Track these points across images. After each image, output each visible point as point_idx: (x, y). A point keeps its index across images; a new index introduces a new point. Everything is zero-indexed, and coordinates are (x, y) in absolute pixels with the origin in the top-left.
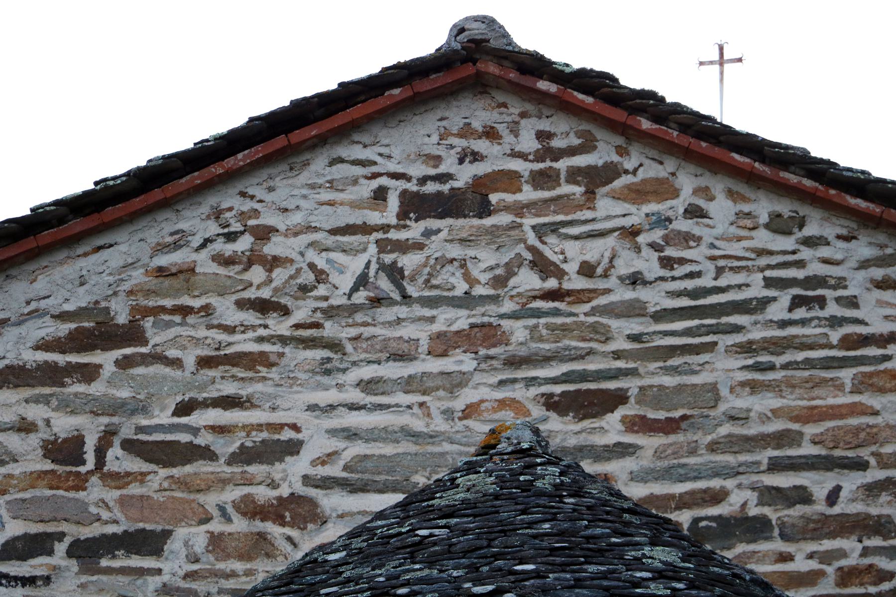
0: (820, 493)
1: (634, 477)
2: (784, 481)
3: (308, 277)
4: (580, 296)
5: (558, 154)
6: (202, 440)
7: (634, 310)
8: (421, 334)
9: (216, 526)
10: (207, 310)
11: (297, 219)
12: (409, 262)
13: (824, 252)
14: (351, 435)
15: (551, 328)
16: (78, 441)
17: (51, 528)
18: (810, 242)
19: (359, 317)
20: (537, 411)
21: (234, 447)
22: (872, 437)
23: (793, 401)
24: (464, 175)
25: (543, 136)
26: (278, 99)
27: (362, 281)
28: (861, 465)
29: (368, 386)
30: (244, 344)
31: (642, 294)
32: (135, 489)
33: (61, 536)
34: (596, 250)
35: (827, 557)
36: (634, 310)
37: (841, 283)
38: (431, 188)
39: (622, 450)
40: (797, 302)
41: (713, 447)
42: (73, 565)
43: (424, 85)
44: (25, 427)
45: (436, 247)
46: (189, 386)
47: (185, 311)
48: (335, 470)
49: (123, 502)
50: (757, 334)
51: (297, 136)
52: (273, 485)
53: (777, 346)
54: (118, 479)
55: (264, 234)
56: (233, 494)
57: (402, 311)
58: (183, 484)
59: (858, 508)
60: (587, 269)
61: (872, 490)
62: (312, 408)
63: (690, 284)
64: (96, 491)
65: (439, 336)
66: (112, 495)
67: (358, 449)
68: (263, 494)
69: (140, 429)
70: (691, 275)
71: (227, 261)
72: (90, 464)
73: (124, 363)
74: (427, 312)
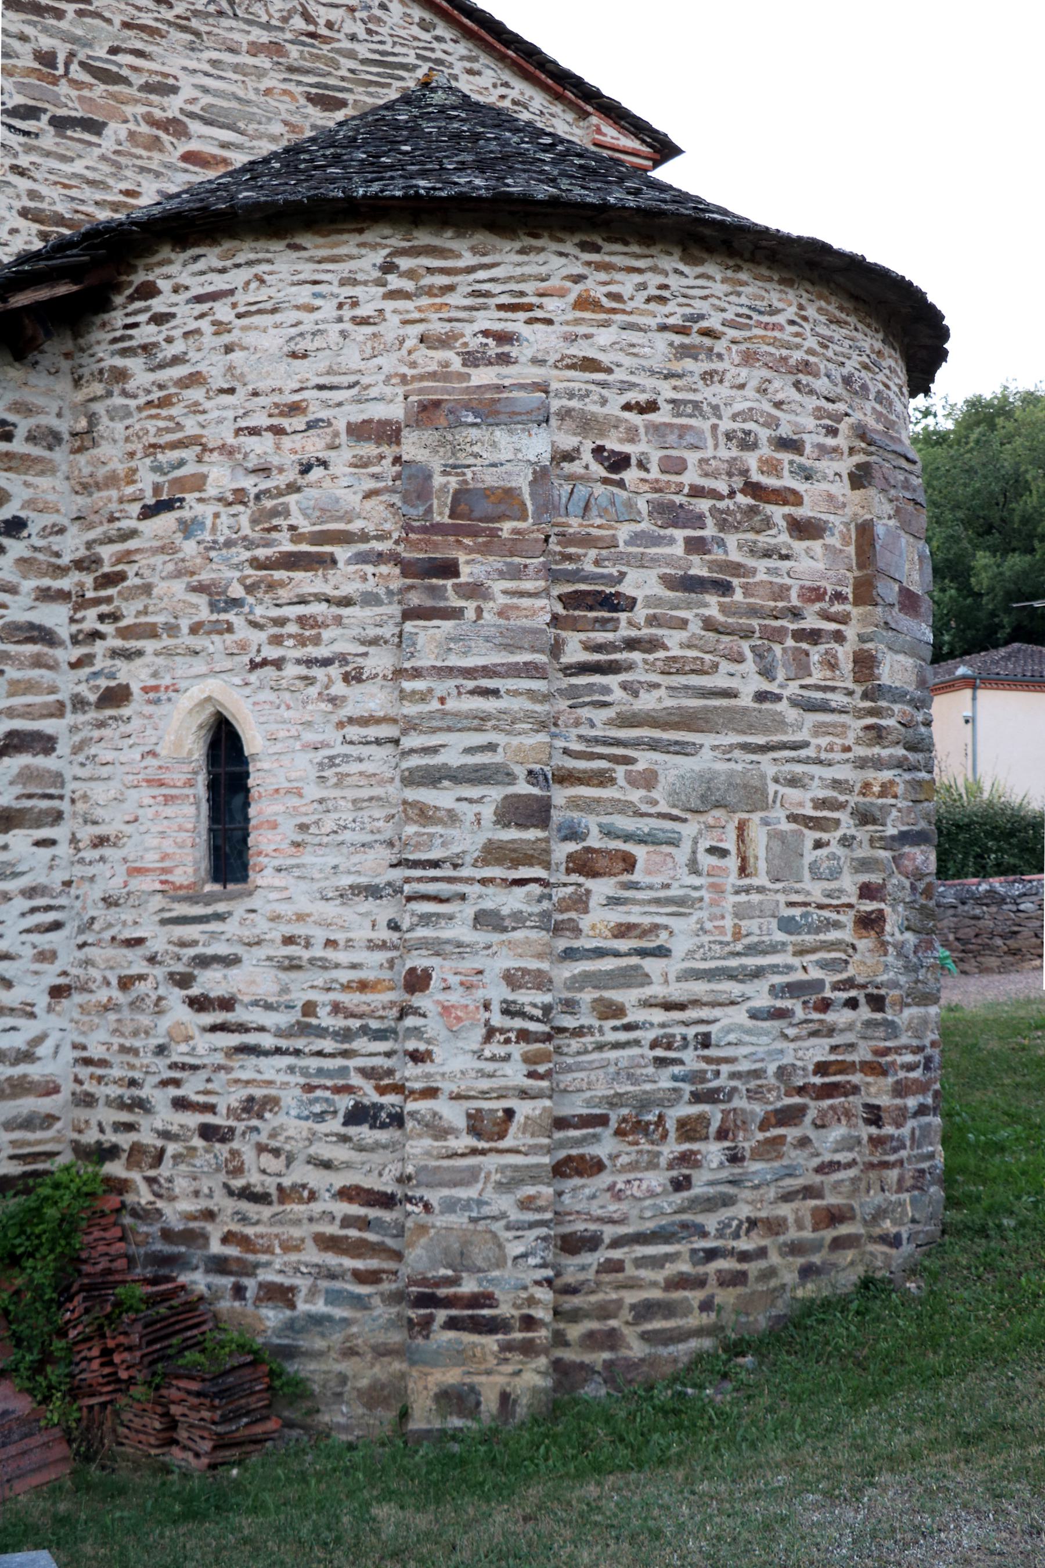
4: (326, 40)
6: (125, 72)
7: (351, 55)
8: (244, 40)
9: (132, 126)
13: (444, 46)
14: (206, 90)
15: (311, 54)
17: (39, 104)
18: (439, 39)
19: (211, 21)
20: (303, 101)
21: (142, 81)
29: (214, 63)
30: (146, 19)
31: (355, 46)
32: (86, 93)
33: (45, 111)
34: (335, 15)
36: (351, 55)
42: (51, 130)
44: (23, 38)
46: (116, 38)
48: (196, 109)
49: (81, 98)
52: (163, 109)
56: (141, 109)
57: (233, 23)
58: (113, 96)
60: (330, 25)
62: (184, 69)
63: (381, 47)
64: (63, 88)
65: (252, 44)
66: (74, 93)
68: (158, 114)
69: (89, 57)
70: (381, 42)
72: (61, 71)
73: (80, 13)
74: (246, 28)
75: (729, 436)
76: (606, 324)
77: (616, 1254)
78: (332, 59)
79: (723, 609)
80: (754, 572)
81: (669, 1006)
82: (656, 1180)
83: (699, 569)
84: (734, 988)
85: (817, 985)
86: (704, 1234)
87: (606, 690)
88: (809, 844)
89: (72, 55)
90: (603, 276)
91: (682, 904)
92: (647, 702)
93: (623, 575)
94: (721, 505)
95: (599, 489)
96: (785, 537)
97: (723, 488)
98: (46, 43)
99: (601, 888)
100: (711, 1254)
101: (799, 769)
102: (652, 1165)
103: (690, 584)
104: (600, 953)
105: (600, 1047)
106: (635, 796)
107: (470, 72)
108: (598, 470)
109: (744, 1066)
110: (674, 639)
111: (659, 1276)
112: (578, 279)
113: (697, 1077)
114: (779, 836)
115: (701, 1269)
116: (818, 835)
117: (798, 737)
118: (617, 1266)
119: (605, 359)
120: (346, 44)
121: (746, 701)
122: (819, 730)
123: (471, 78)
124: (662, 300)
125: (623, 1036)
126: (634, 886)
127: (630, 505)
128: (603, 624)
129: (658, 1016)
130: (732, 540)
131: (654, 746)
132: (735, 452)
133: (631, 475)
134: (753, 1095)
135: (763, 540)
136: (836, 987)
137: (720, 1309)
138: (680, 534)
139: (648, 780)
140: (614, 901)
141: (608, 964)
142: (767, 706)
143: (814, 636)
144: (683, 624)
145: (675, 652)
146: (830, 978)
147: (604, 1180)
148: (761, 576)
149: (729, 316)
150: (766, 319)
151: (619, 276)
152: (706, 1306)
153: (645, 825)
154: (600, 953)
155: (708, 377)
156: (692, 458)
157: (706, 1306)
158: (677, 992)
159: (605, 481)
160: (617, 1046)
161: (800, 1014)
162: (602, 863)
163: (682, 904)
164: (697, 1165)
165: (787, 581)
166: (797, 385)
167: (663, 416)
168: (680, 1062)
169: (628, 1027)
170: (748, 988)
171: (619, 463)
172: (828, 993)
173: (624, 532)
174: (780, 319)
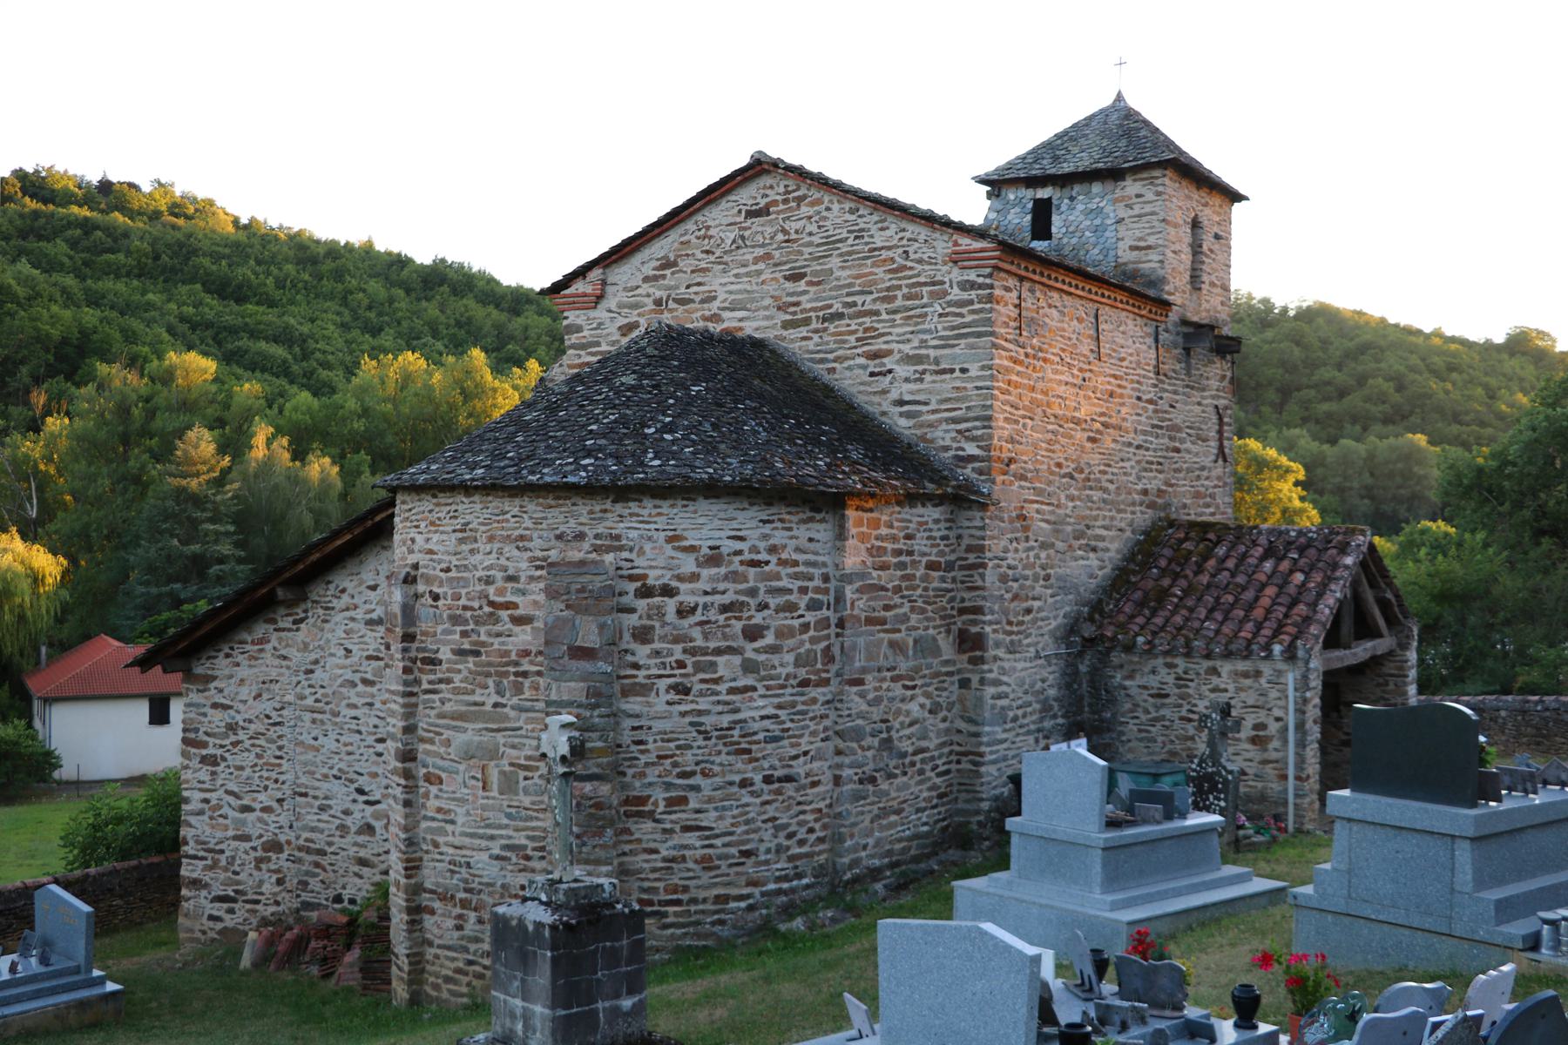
0: (860, 303)
1: (809, 301)
2: (849, 299)
3: (719, 241)
4: (795, 241)
5: (789, 193)
6: (692, 297)
7: (810, 244)
8: (749, 257)
10: (693, 254)
11: (717, 222)
12: (747, 233)
13: (864, 219)
14: (731, 292)
16: (661, 299)
18: (860, 216)
20: (782, 281)
22: (875, 283)
23: (854, 272)
24: (763, 202)
25: (786, 186)
26: (703, 186)
27: (734, 241)
28: (871, 293)
29: (736, 276)
32: (675, 314)
34: (799, 225)
35: (860, 324)
36: (810, 244)
37: (869, 230)
38: (754, 208)
39: (805, 292)
41: (830, 290)
43: (747, 175)
44: (648, 295)
45: (755, 228)
47: (687, 255)
48: (726, 305)
50: (844, 250)
51: (713, 196)
53: (849, 253)
54: (671, 311)
55: (708, 228)
57: (745, 250)
58: (686, 311)
59: (870, 307)
60: (797, 232)
61: (875, 300)
66: (669, 316)
67: (733, 297)
68: (707, 313)
71: (698, 238)
73: (673, 273)
75: (480, 580)
76: (436, 532)
77: (439, 951)
78: (799, 251)
79: (475, 664)
80: (492, 644)
81: (456, 848)
82: (450, 923)
83: (467, 646)
84: (484, 843)
85: (525, 847)
86: (468, 953)
87: (434, 702)
88: (521, 778)
89: (669, 296)
90: (437, 509)
91: (462, 801)
92: (448, 707)
93: (438, 649)
94: (476, 613)
95: (432, 610)
96: (509, 626)
97: (476, 604)
98: (658, 294)
99: (434, 790)
100: (470, 963)
101: (516, 740)
102: (450, 917)
103: (461, 653)
104: (433, 819)
105: (433, 860)
106: (442, 750)
107: (882, 229)
108: (430, 601)
109: (485, 880)
110: (457, 678)
111: (453, 965)
112: (430, 511)
113: (466, 881)
114: (503, 773)
115: (467, 968)
116: (527, 773)
117: (517, 725)
118: (437, 957)
119: (435, 548)
120: (808, 239)
121: (488, 708)
122: (527, 722)
123: (882, 233)
124: (456, 517)
125: (439, 857)
126: (441, 790)
127: (441, 615)
128: (433, 672)
129: (451, 851)
130: (482, 630)
131: (448, 727)
132: (483, 587)
133: (440, 603)
134: (491, 894)
135: (498, 628)
136: (534, 849)
137: (474, 988)
138: (458, 629)
139: (448, 743)
140: (437, 797)
141: (434, 824)
142: (498, 710)
143: (525, 674)
144: (459, 671)
145: (457, 685)
146: (531, 844)
147: (436, 918)
148: (496, 646)
149: (481, 520)
150: (501, 518)
151: (443, 508)
152: (469, 984)
153: (446, 764)
154: (433, 819)
155: (472, 551)
156: (463, 592)
157: (469, 984)
158: (457, 841)
159: (432, 606)
160: (438, 861)
161: (514, 860)
162: (433, 779)
163: (462, 801)
164: (466, 921)
165: (510, 647)
166: (518, 548)
167: (453, 574)
168: (459, 873)
169: (441, 854)
170: (490, 844)
171: (436, 597)
172: (529, 852)
173: (440, 629)
174: (508, 516)
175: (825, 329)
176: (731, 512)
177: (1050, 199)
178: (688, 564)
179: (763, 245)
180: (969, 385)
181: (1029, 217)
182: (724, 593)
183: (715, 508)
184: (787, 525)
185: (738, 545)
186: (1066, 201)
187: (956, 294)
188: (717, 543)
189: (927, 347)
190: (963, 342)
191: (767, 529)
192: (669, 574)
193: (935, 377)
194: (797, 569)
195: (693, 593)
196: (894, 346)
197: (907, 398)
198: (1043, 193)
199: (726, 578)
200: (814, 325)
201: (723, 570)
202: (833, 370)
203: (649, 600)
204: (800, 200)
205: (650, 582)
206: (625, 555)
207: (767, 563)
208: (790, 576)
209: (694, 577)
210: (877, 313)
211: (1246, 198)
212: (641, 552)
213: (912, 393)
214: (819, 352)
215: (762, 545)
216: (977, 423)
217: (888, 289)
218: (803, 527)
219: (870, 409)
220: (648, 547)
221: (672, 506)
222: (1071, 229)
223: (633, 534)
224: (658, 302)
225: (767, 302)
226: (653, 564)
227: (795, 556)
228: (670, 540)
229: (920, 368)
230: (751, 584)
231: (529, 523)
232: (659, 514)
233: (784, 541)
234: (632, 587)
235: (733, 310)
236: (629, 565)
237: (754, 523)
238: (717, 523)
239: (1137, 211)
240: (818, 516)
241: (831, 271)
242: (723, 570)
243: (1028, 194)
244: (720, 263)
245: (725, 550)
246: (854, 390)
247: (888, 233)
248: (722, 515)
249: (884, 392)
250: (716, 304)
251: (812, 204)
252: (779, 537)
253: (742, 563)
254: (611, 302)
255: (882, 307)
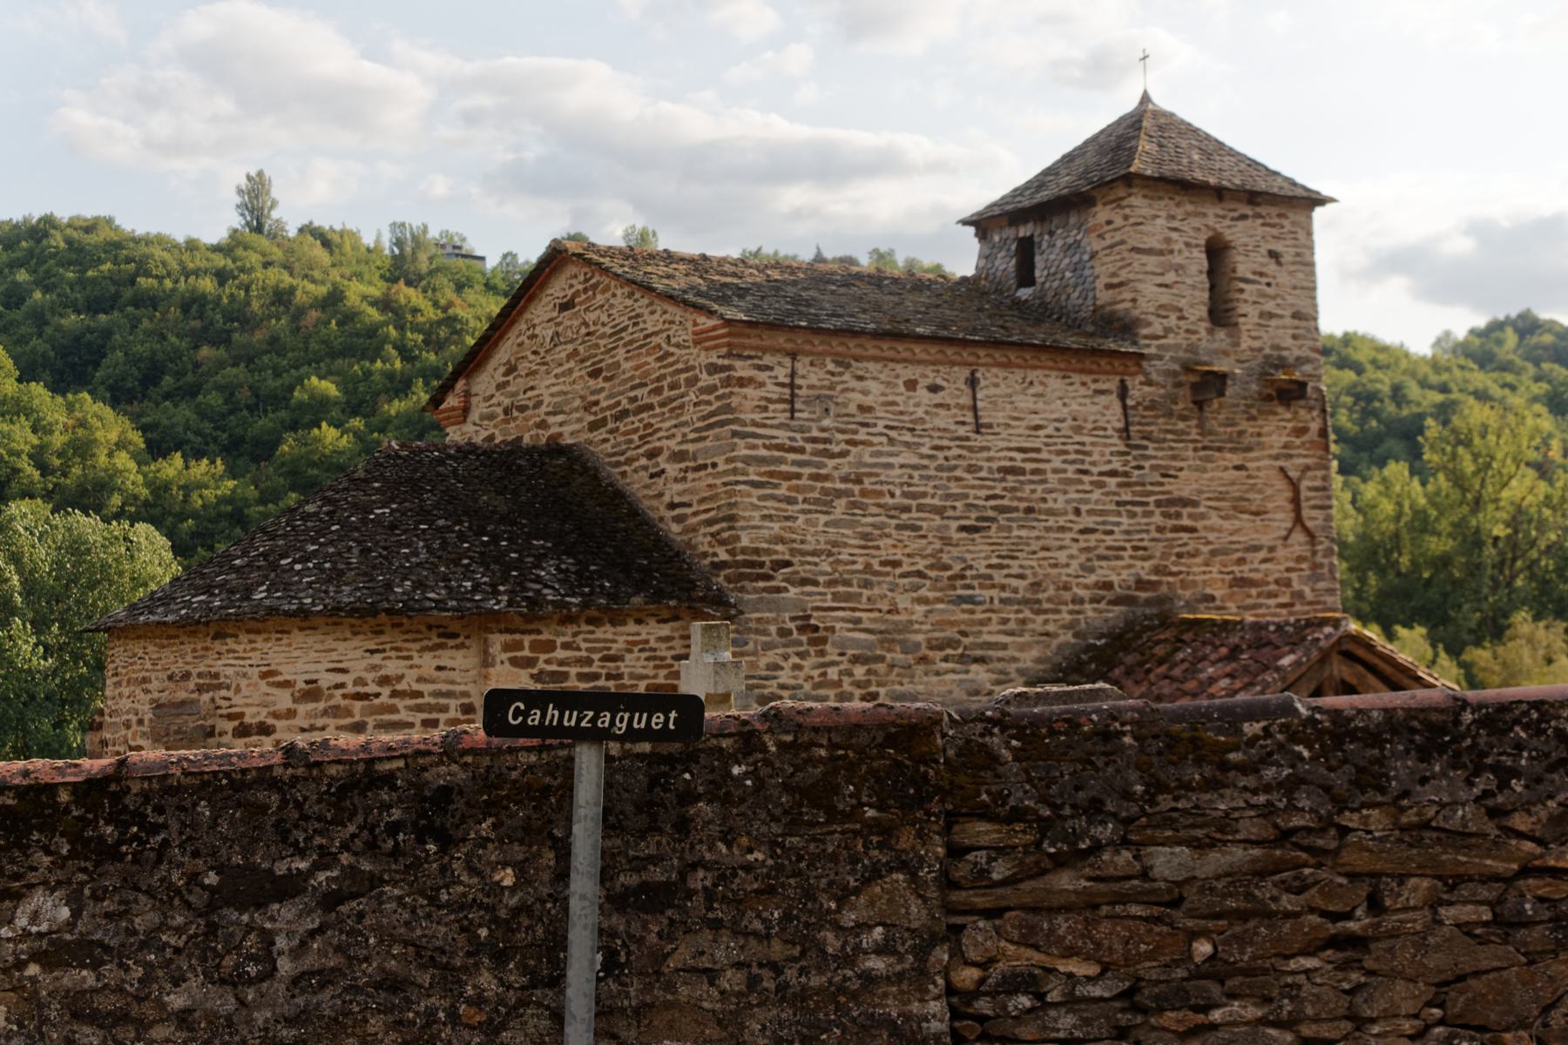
2: (632, 394)
7: (603, 336)
8: (563, 355)
12: (560, 329)
24: (570, 293)
28: (646, 385)
29: (556, 376)
40: (635, 324)
53: (631, 342)
60: (595, 324)
107: (652, 313)
175: (617, 429)
176: (330, 643)
177: (1032, 236)
178: (284, 700)
179: (572, 341)
180: (718, 482)
181: (1014, 261)
182: (323, 729)
183: (310, 640)
184: (405, 654)
185: (340, 678)
186: (1046, 237)
187: (706, 380)
188: (314, 677)
189: (687, 442)
190: (711, 433)
191: (376, 659)
192: (264, 712)
193: (697, 475)
194: (420, 701)
195: (289, 729)
196: (665, 443)
197: (677, 500)
198: (1024, 231)
199: (325, 713)
200: (611, 425)
201: (321, 705)
202: (624, 474)
203: (247, 740)
204: (595, 287)
205: (247, 720)
206: (224, 693)
207: (377, 695)
208: (409, 708)
209: (291, 714)
210: (650, 407)
211: (1332, 200)
212: (238, 690)
213: (679, 494)
214: (614, 454)
215: (370, 677)
216: (724, 525)
217: (658, 379)
218: (428, 656)
219: (651, 514)
220: (243, 683)
221: (266, 640)
222: (1053, 270)
223: (230, 671)
224: (507, 411)
225: (578, 402)
226: (249, 701)
227: (416, 687)
228: (264, 676)
229: (683, 465)
230: (357, 718)
231: (148, 666)
232: (254, 649)
233: (400, 672)
234: (229, 726)
235: (554, 414)
236: (227, 703)
237: (359, 653)
238: (313, 655)
239: (1108, 242)
240: (451, 642)
241: (618, 364)
242: (321, 705)
243: (1010, 232)
244: (544, 364)
245: (324, 684)
246: (640, 495)
247: (656, 316)
248: (319, 646)
249: (660, 495)
250: (544, 409)
251: (604, 291)
252: (392, 667)
253: (344, 696)
254: (475, 415)
255: (655, 400)
